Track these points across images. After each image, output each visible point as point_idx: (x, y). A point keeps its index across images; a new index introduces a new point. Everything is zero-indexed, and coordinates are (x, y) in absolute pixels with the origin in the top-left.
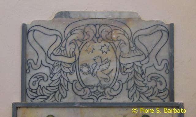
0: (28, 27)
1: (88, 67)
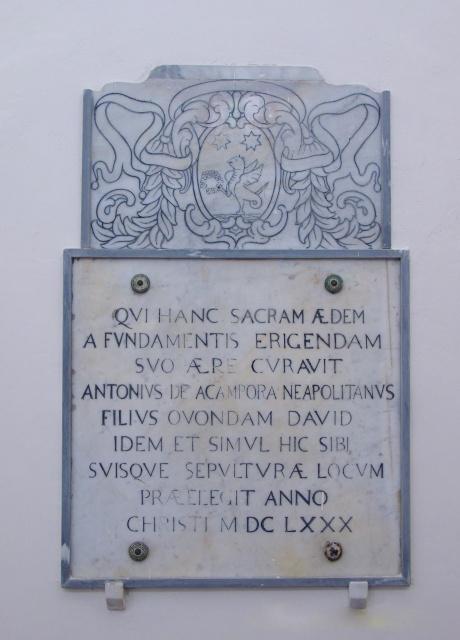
0: (96, 97)
1: (219, 178)
